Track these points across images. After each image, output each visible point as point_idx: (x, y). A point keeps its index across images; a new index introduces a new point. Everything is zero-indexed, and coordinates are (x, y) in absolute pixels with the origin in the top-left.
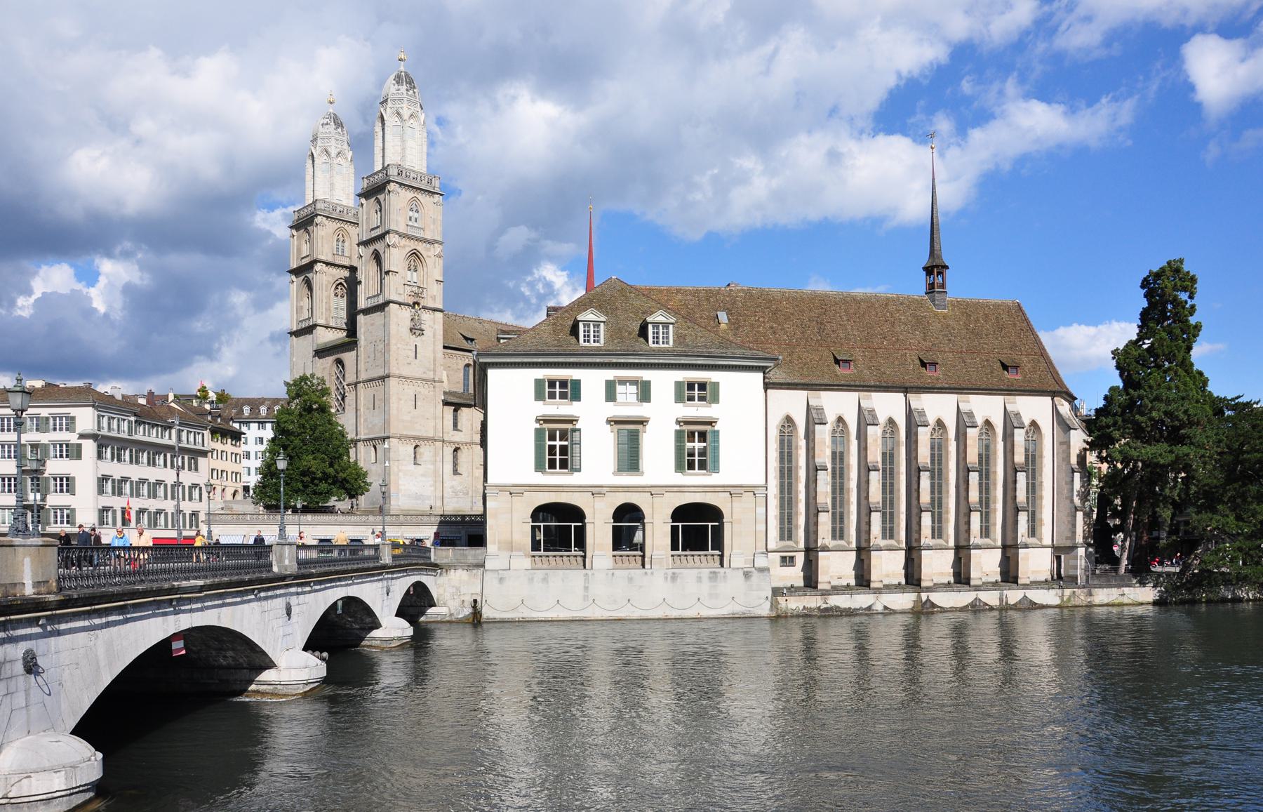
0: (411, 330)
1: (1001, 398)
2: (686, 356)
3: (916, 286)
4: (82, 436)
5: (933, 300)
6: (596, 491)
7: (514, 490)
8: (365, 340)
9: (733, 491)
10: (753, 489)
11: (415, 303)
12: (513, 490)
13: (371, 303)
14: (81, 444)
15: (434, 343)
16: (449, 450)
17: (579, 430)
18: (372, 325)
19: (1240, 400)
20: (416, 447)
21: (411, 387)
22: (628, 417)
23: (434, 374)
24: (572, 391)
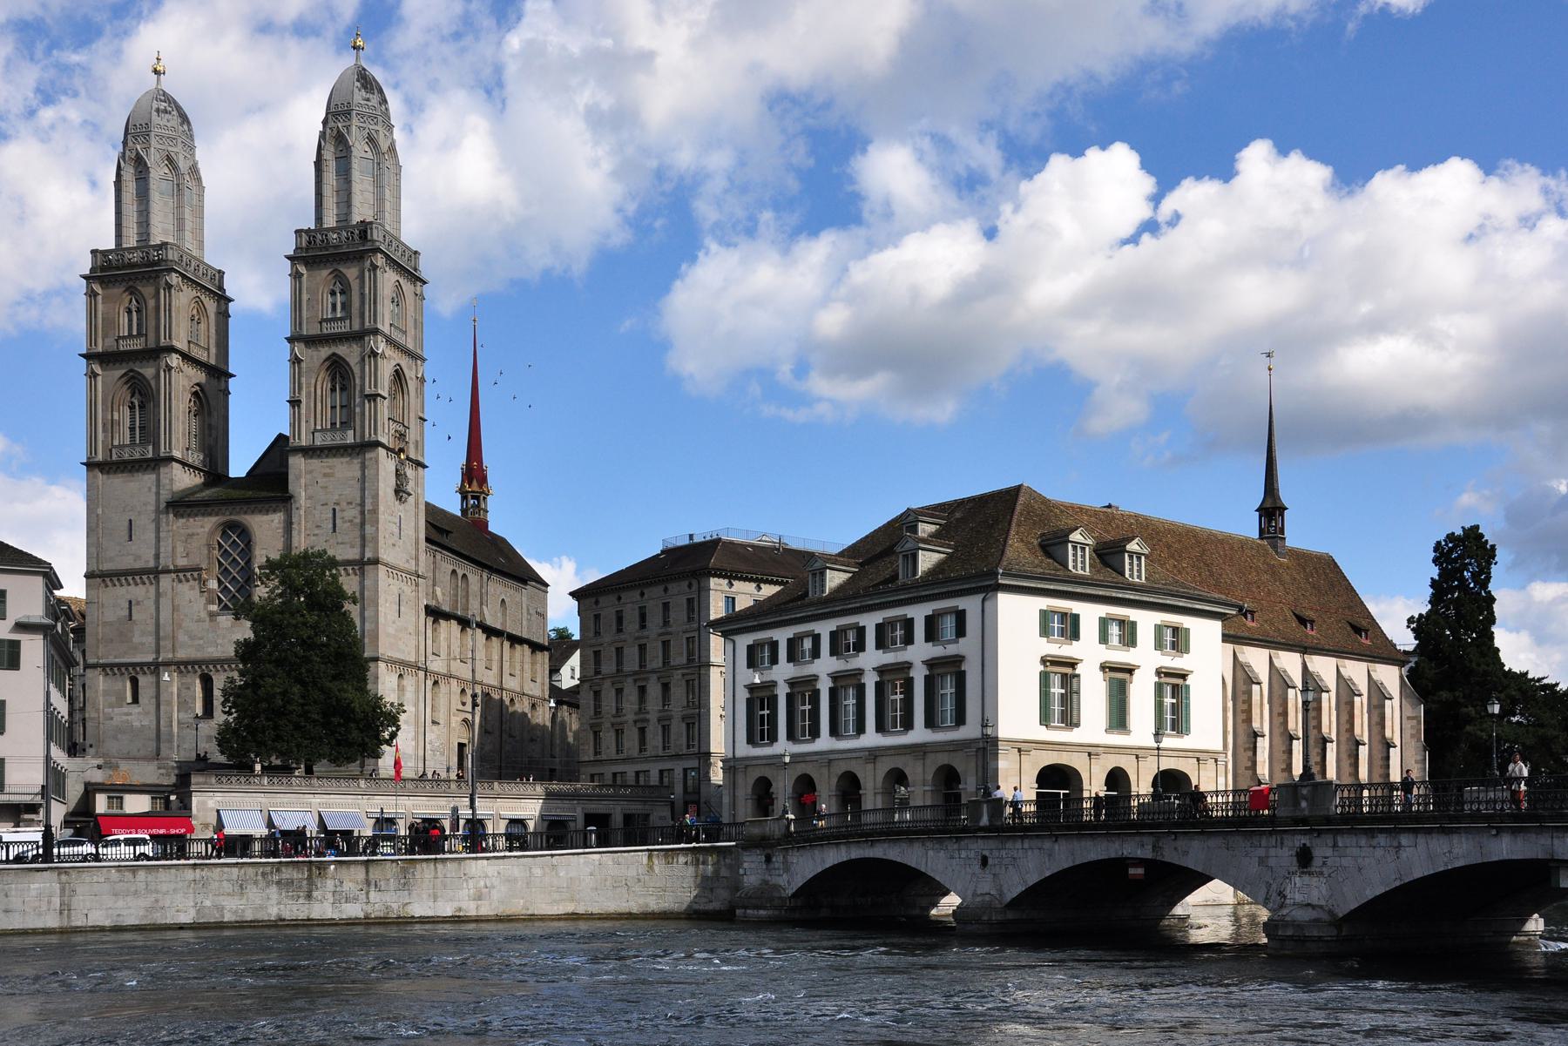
0: (397, 492)
1: (1334, 660)
2: (1173, 596)
3: (1247, 526)
4: (21, 627)
5: (1275, 547)
6: (1092, 751)
7: (1022, 747)
8: (309, 498)
9: (1199, 756)
10: (1197, 755)
11: (402, 450)
12: (1023, 746)
13: (319, 441)
14: (18, 642)
15: (417, 515)
16: (430, 683)
17: (1078, 676)
18: (325, 475)
19: (1545, 681)
20: (400, 676)
21: (395, 580)
22: (1121, 664)
23: (417, 565)
24: (1071, 628)
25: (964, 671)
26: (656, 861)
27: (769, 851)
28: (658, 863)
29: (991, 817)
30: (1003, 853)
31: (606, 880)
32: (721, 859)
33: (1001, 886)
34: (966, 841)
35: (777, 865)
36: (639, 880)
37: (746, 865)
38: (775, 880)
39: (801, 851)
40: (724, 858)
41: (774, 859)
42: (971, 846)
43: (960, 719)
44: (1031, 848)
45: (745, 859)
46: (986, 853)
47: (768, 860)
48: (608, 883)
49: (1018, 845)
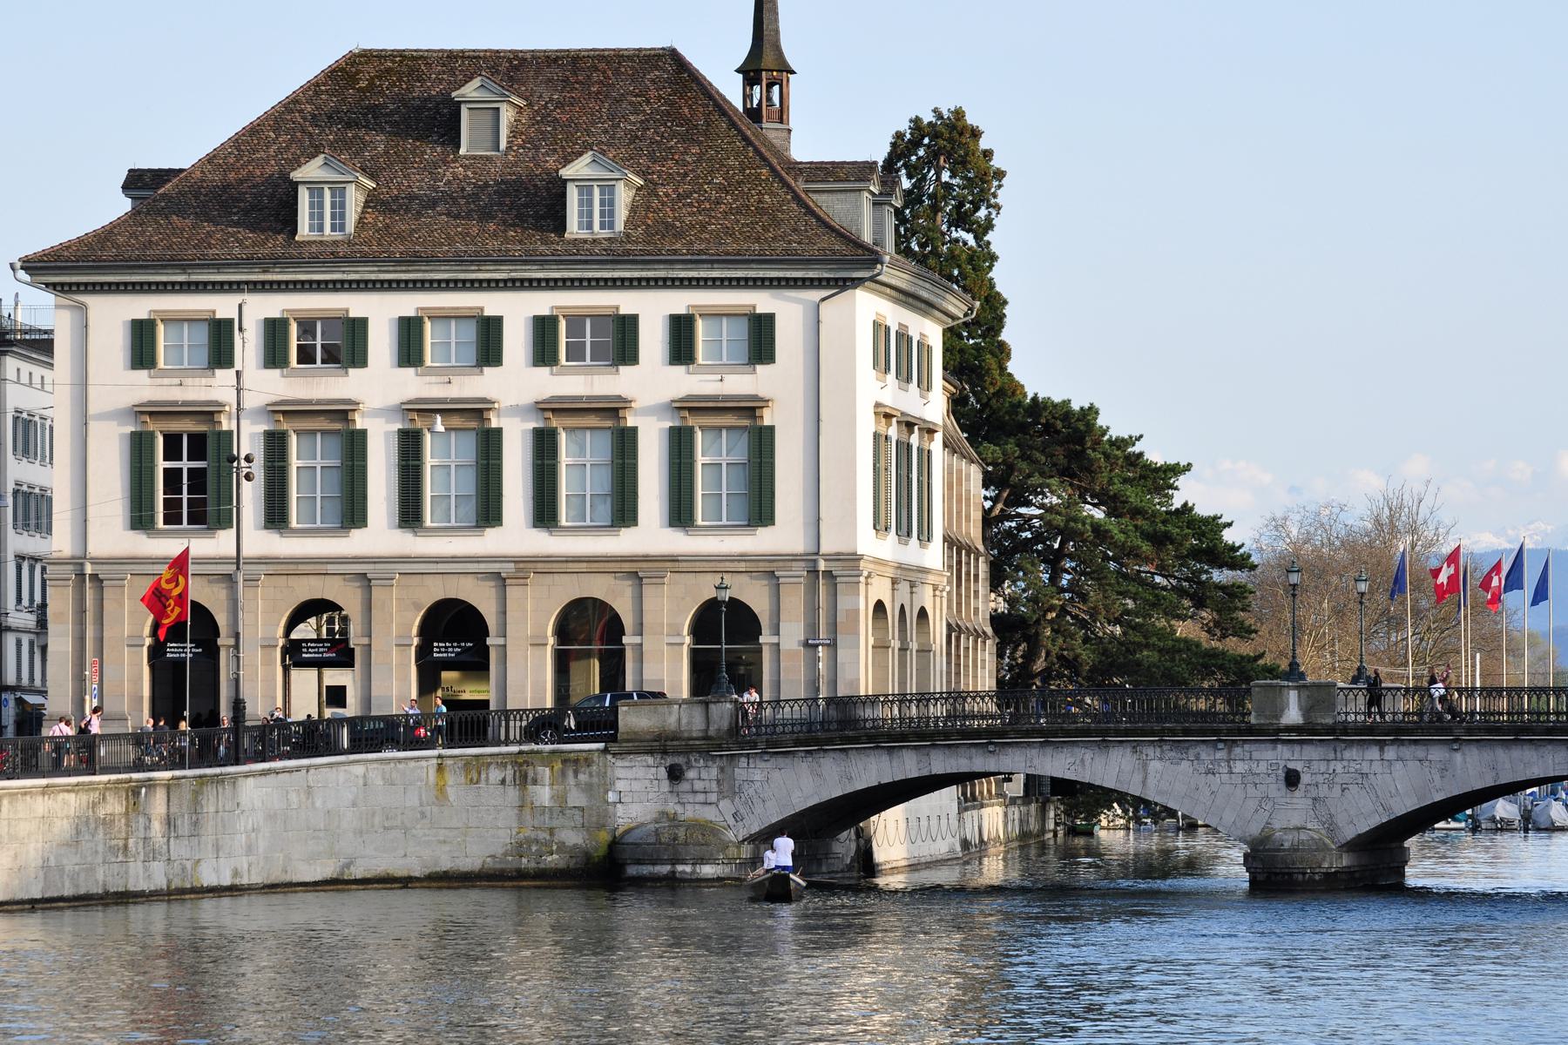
25: (771, 429)
26: (450, 779)
27: (680, 760)
28: (453, 780)
29: (1307, 711)
30: (1339, 767)
31: (373, 814)
32: (570, 773)
33: (1331, 816)
34: (1247, 747)
35: (698, 785)
36: (423, 816)
37: (620, 785)
38: (689, 813)
39: (781, 761)
40: (576, 773)
41: (691, 774)
42: (1256, 755)
43: (760, 511)
44: (1399, 759)
45: (620, 773)
46: (1298, 766)
47: (675, 774)
48: (377, 820)
49: (1373, 753)
